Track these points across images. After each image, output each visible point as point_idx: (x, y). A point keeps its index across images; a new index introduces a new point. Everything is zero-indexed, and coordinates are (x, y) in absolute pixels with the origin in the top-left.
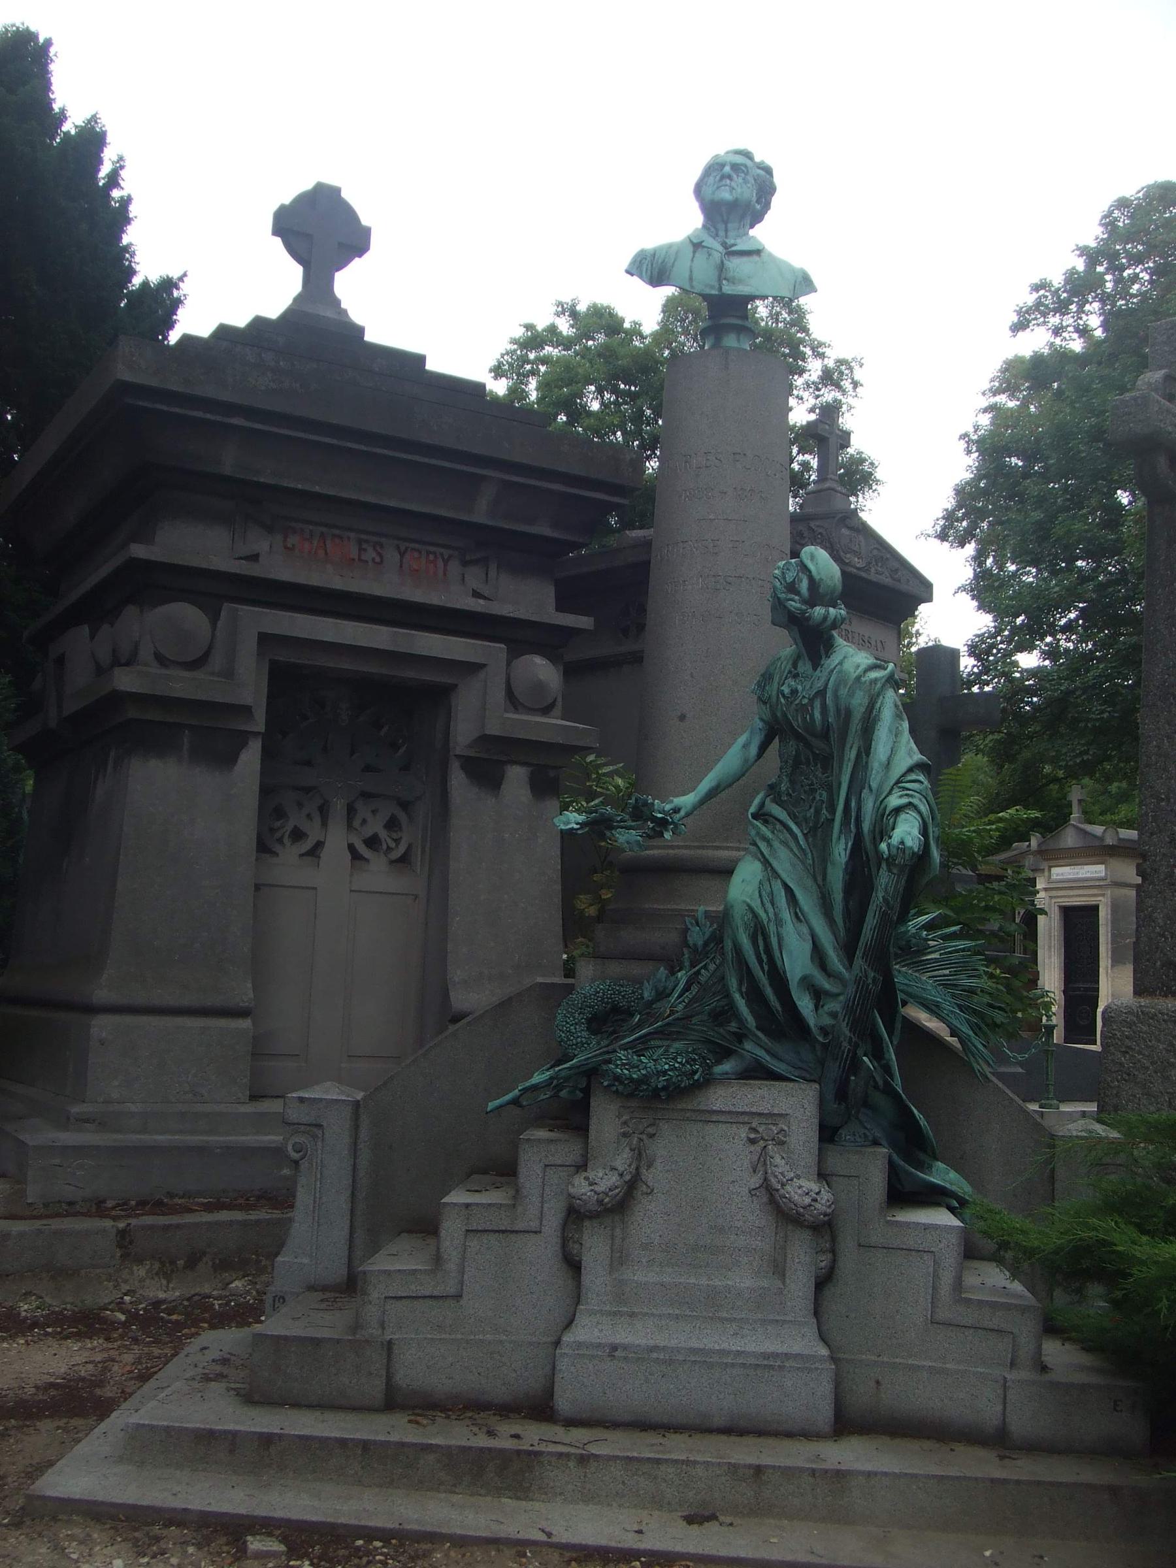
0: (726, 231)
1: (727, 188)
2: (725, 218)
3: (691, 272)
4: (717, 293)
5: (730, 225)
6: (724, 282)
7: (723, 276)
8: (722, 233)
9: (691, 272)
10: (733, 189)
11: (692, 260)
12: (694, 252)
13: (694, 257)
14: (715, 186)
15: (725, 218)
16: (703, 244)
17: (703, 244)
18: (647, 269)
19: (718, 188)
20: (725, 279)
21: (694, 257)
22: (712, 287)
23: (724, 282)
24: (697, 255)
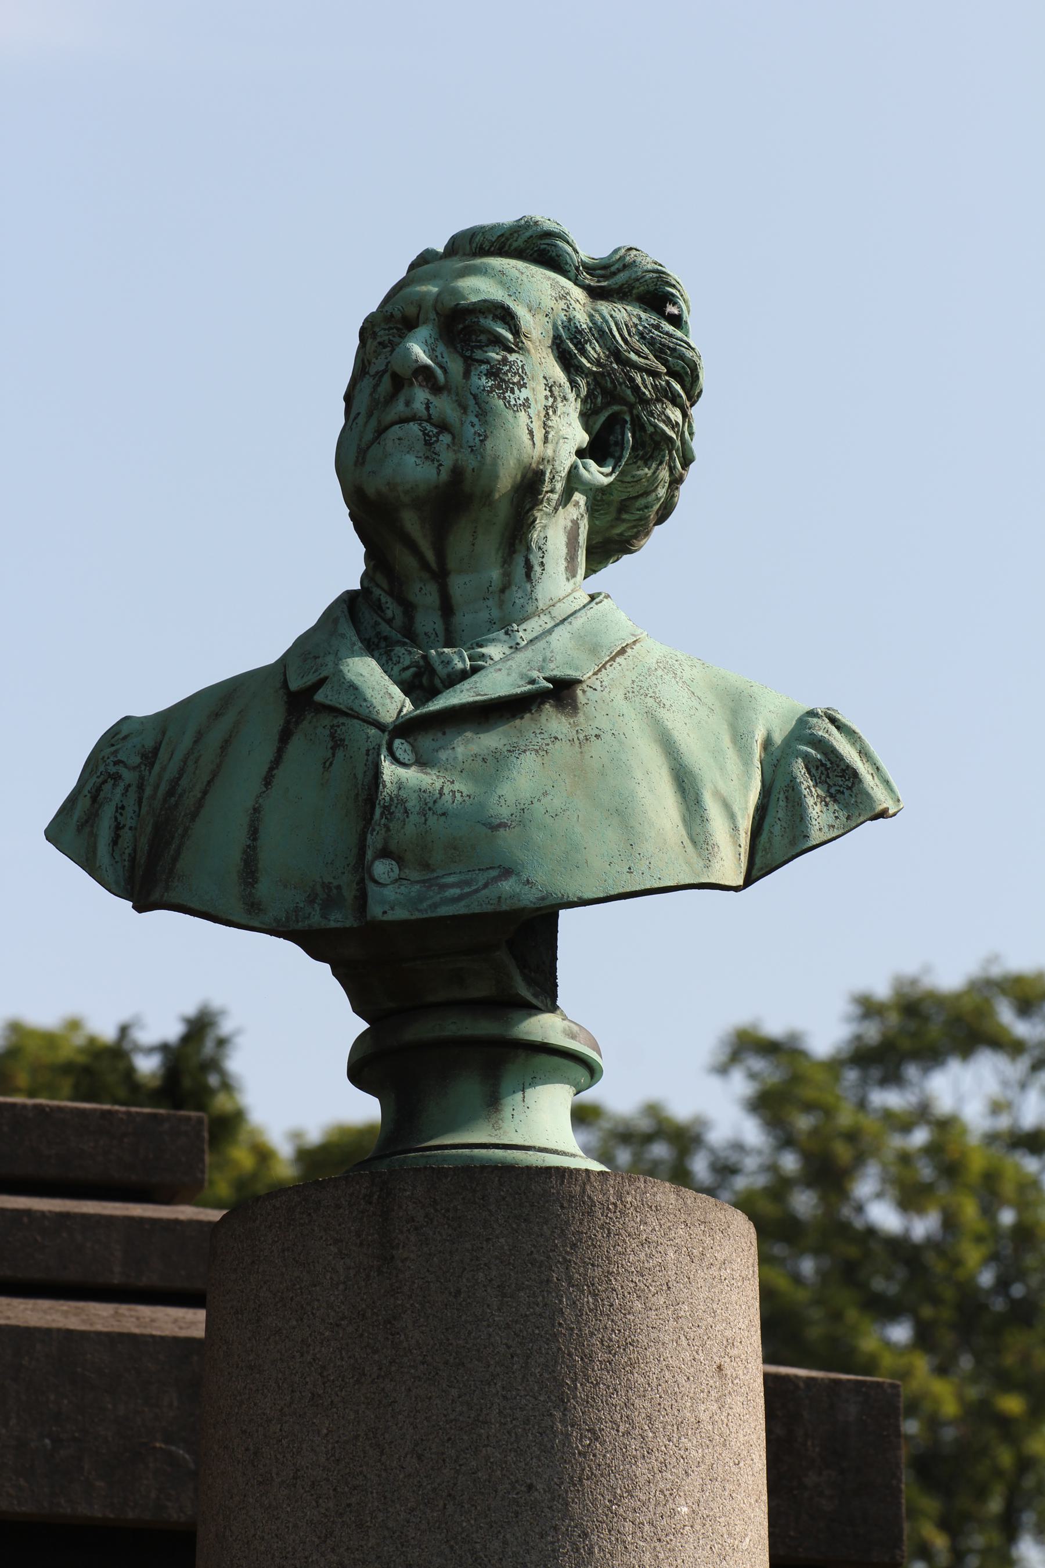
0: (447, 609)
1: (414, 427)
2: (430, 556)
3: (254, 833)
4: (350, 922)
5: (460, 585)
6: (382, 869)
7: (374, 841)
8: (428, 621)
9: (254, 833)
10: (444, 427)
11: (268, 781)
12: (285, 736)
13: (277, 761)
14: (373, 423)
15: (430, 556)
16: (320, 697)
17: (320, 697)
18: (118, 827)
19: (381, 431)
20: (385, 853)
21: (277, 761)
22: (330, 901)
23: (382, 869)
24: (297, 745)
